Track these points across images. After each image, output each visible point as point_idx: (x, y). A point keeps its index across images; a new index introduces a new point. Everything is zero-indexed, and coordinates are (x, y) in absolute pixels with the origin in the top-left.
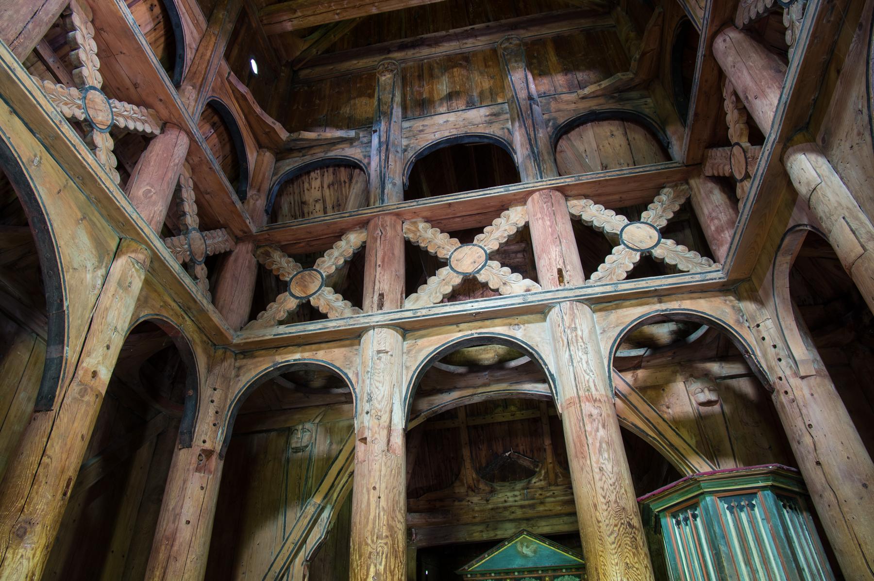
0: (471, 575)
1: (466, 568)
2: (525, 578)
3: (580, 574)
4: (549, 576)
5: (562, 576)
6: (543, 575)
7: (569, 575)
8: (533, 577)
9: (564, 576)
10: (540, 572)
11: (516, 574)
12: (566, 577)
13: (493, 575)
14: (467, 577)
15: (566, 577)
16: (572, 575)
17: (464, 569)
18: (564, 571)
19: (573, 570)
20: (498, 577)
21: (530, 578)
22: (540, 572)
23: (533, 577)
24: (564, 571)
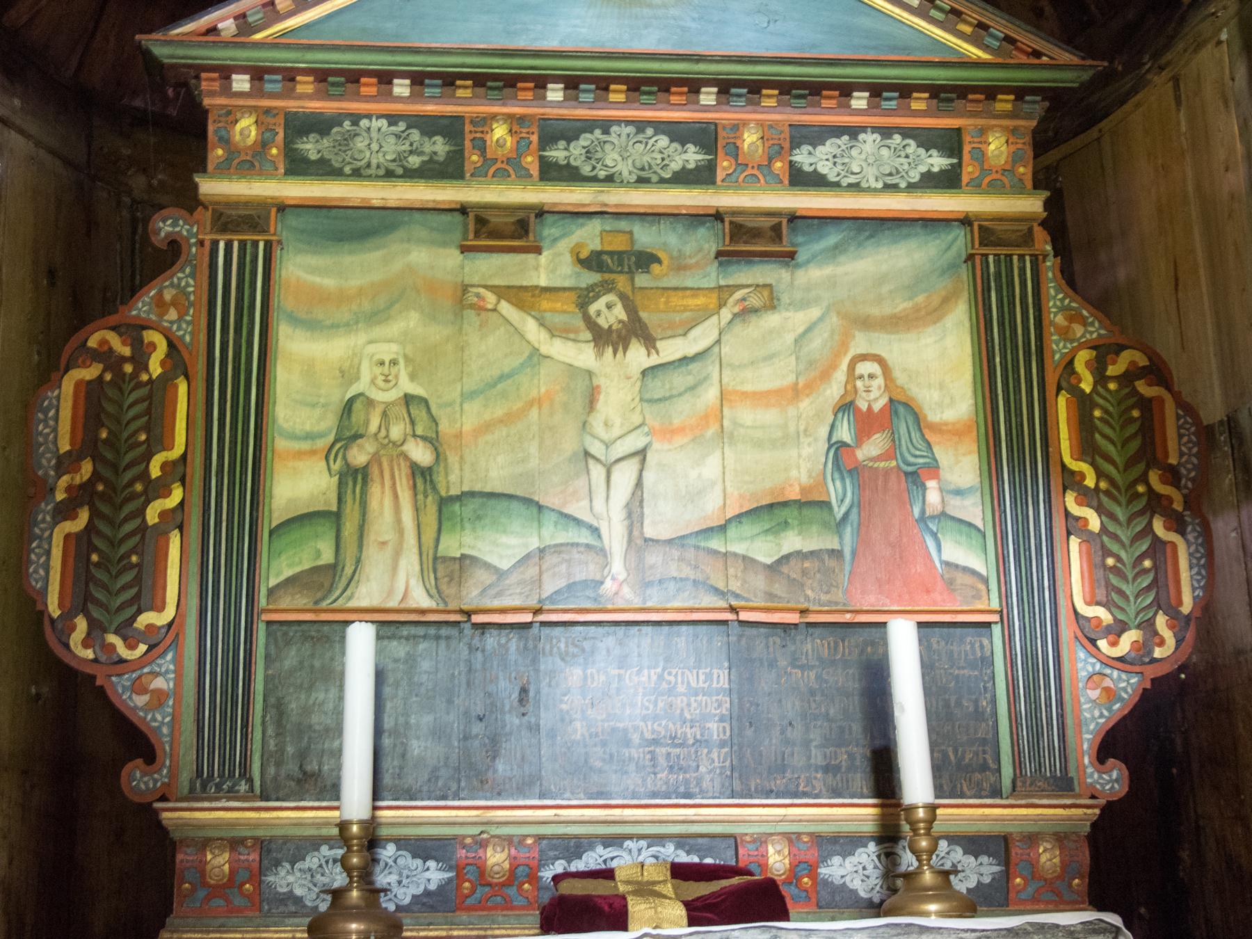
0: (258, 74)
1: (228, 26)
2: (605, 126)
3: (959, 130)
4: (760, 124)
5: (838, 131)
6: (725, 116)
7: (886, 132)
8: (661, 127)
9: (854, 132)
10: (708, 97)
11: (555, 93)
12: (869, 140)
13: (401, 88)
14: (227, 90)
15: (869, 140)
16: (906, 133)
17: (213, 30)
18: (860, 101)
19: (919, 103)
20: (431, 108)
21: (640, 126)
22: (708, 97)
23: (661, 127)
24: (860, 101)
